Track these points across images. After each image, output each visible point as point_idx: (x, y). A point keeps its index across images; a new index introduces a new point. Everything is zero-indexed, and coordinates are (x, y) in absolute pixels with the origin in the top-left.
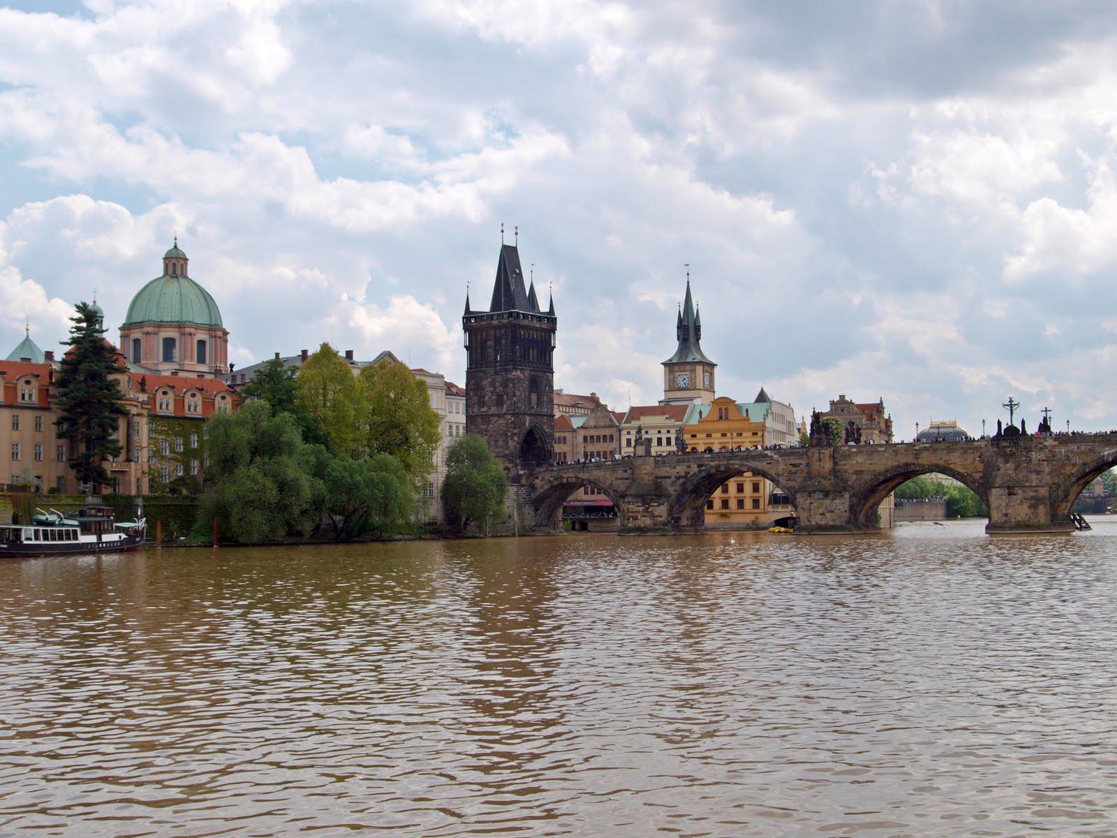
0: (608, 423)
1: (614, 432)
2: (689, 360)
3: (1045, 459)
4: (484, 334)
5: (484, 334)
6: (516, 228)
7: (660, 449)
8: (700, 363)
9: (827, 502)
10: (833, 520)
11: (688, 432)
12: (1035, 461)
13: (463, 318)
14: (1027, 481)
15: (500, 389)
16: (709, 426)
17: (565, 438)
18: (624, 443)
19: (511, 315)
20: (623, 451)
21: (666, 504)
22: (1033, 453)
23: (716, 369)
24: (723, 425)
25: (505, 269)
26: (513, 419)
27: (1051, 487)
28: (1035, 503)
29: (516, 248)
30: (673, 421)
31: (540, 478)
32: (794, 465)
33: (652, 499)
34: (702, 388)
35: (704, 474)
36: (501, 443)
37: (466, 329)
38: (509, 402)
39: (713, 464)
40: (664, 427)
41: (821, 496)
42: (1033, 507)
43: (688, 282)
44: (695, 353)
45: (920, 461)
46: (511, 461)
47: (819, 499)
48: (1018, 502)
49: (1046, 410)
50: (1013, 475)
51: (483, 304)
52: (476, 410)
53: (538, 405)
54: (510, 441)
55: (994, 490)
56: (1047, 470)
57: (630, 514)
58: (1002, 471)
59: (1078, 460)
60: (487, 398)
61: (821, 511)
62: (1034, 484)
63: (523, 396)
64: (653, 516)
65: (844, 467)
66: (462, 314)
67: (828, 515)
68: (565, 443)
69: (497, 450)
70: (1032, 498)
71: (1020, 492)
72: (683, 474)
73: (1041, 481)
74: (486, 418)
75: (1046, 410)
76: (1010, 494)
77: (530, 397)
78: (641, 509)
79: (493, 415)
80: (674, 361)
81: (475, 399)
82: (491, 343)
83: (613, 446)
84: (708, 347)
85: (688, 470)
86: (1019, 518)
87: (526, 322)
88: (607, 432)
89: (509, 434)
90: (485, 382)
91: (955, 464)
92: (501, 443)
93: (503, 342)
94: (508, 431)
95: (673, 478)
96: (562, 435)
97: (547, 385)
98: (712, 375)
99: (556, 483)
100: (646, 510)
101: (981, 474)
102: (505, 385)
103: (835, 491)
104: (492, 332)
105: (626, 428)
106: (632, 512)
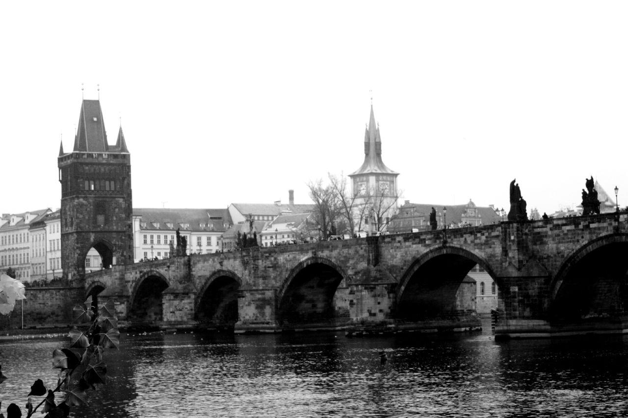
2: (366, 172)
3: (271, 266)
8: (372, 174)
9: (176, 302)
10: (182, 317)
12: (261, 268)
14: (254, 286)
21: (126, 303)
22: (260, 261)
23: (398, 177)
27: (276, 290)
33: (115, 299)
35: (143, 279)
36: (73, 255)
40: (285, 233)
41: (172, 297)
42: (260, 307)
43: (372, 106)
45: (224, 268)
47: (170, 300)
48: (247, 303)
50: (248, 280)
53: (105, 224)
54: (76, 253)
56: (273, 275)
59: (289, 266)
61: (171, 310)
62: (261, 288)
63: (87, 218)
67: (177, 313)
70: (259, 299)
71: (248, 294)
73: (267, 286)
79: (70, 233)
84: (390, 160)
86: (247, 317)
87: (89, 160)
89: (75, 248)
91: (237, 270)
97: (116, 208)
98: (392, 182)
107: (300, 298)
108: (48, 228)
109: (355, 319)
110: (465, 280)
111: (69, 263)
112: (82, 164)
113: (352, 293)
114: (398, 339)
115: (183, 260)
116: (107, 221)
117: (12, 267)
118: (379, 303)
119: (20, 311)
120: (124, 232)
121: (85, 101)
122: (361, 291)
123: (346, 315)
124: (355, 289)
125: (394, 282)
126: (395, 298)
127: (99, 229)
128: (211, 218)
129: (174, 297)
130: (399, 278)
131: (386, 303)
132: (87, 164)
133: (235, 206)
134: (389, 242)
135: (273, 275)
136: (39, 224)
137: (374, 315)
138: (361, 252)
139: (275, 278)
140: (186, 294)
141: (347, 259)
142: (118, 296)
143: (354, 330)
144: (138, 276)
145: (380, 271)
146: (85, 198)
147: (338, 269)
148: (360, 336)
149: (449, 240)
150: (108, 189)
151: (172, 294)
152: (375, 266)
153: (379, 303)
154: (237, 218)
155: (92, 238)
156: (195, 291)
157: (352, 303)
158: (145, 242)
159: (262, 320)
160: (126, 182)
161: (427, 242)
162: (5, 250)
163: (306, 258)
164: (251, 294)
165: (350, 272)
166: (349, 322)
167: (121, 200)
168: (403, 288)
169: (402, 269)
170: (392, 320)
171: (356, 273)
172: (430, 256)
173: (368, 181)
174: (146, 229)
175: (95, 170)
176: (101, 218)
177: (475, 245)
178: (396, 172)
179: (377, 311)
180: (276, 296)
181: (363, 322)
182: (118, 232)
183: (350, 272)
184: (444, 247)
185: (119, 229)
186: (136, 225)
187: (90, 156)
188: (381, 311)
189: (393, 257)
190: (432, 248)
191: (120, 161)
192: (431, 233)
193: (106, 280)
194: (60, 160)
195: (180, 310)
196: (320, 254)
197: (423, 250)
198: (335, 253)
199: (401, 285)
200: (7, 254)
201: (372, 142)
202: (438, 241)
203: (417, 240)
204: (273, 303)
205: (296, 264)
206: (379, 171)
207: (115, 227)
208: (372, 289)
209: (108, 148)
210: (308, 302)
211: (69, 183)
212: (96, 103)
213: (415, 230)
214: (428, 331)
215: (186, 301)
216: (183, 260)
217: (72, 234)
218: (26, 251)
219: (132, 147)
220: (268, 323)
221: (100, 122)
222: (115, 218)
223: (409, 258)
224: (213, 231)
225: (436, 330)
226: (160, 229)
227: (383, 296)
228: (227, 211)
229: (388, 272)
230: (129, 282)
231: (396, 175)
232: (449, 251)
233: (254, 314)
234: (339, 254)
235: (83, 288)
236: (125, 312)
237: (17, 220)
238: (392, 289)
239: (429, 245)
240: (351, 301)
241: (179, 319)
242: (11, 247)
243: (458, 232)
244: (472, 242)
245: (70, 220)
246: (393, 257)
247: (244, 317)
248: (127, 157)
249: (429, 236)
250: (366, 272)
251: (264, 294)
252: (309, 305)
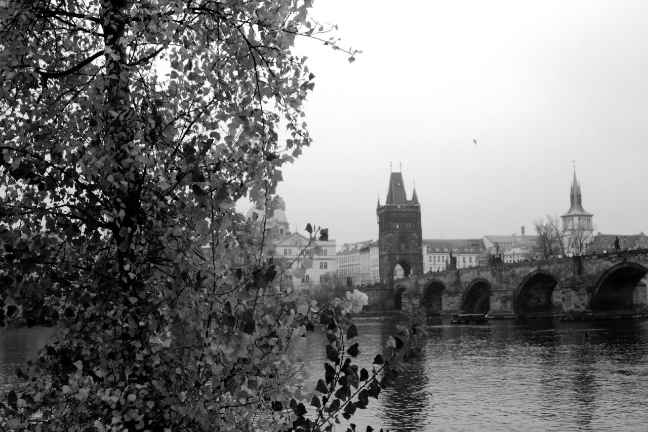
2: (572, 214)
8: (576, 215)
9: (450, 298)
14: (500, 288)
22: (504, 272)
23: (593, 217)
37: (378, 214)
45: (481, 277)
51: (383, 203)
53: (406, 250)
59: (522, 275)
62: (504, 289)
66: (376, 207)
67: (451, 305)
70: (503, 297)
71: (496, 294)
77: (400, 246)
84: (587, 205)
86: (496, 308)
97: (412, 239)
98: (589, 220)
100: (410, 302)
105: (507, 255)
107: (531, 296)
108: (371, 252)
109: (566, 309)
110: (639, 284)
112: (391, 212)
113: (564, 292)
114: (596, 322)
116: (407, 247)
117: (350, 276)
118: (582, 299)
120: (417, 254)
122: (570, 292)
123: (560, 307)
124: (566, 290)
125: (591, 285)
126: (592, 296)
128: (472, 245)
130: (595, 283)
131: (586, 299)
132: (394, 212)
133: (487, 237)
134: (588, 260)
135: (512, 281)
136: (366, 249)
137: (579, 307)
138: (570, 266)
139: (513, 283)
140: (456, 293)
141: (560, 270)
143: (565, 317)
144: (426, 281)
145: (582, 278)
146: (393, 233)
147: (554, 277)
148: (569, 320)
149: (628, 258)
150: (407, 227)
152: (579, 275)
153: (582, 299)
154: (488, 245)
155: (398, 258)
156: (462, 291)
157: (563, 299)
158: (430, 260)
159: (505, 310)
160: (418, 223)
161: (613, 259)
162: (346, 266)
163: (533, 270)
165: (562, 279)
166: (562, 311)
167: (415, 235)
168: (597, 289)
170: (590, 311)
171: (566, 280)
172: (616, 268)
173: (573, 220)
174: (431, 252)
176: (403, 246)
177: (646, 261)
178: (591, 214)
179: (580, 305)
180: (514, 294)
181: (571, 312)
182: (413, 254)
183: (562, 279)
184: (625, 262)
185: (415, 253)
186: (425, 250)
188: (583, 304)
189: (591, 269)
190: (616, 263)
191: (414, 210)
192: (616, 253)
193: (407, 284)
194: (378, 210)
195: (453, 303)
196: (542, 268)
197: (611, 265)
198: (552, 267)
199: (596, 287)
200: (347, 268)
201: (575, 194)
202: (620, 259)
203: (606, 258)
204: (512, 299)
205: (527, 274)
206: (580, 214)
208: (576, 290)
209: (407, 202)
210: (535, 298)
213: (605, 252)
214: (615, 317)
215: (456, 298)
217: (385, 255)
218: (358, 266)
219: (421, 201)
220: (509, 312)
221: (402, 186)
223: (601, 270)
224: (473, 253)
225: (620, 317)
226: (439, 252)
227: (584, 295)
228: (482, 241)
229: (587, 279)
230: (420, 285)
231: (591, 216)
232: (628, 265)
234: (555, 267)
235: (393, 289)
236: (418, 303)
237: (353, 247)
238: (590, 290)
239: (614, 262)
240: (563, 298)
241: (452, 309)
242: (349, 263)
243: (634, 253)
244: (644, 259)
246: (591, 269)
248: (418, 208)
249: (614, 256)
250: (573, 279)
251: (506, 293)
252: (536, 301)
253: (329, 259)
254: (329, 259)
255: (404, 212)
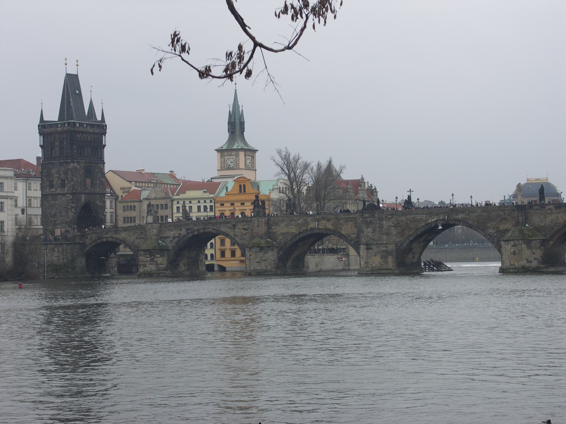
0: (164, 195)
1: (168, 202)
2: (235, 147)
4: (53, 137)
5: (53, 137)
6: (77, 61)
7: (199, 214)
8: (242, 149)
9: (260, 254)
10: (266, 266)
11: (218, 202)
13: (39, 126)
14: (380, 240)
15: (63, 176)
16: (232, 198)
17: (135, 207)
18: (175, 210)
19: (69, 123)
20: (174, 215)
22: (385, 221)
24: (242, 197)
25: (68, 91)
26: (71, 197)
28: (385, 255)
29: (77, 76)
30: (208, 194)
31: (89, 238)
32: (245, 229)
34: (244, 168)
35: (190, 235)
36: (64, 214)
37: (40, 134)
38: (69, 185)
39: (195, 228)
41: (258, 250)
43: (236, 90)
44: (239, 142)
46: (70, 227)
47: (256, 252)
48: (374, 254)
49: (410, 191)
51: (52, 115)
52: (47, 190)
53: (91, 188)
54: (70, 213)
55: (362, 246)
57: (141, 263)
58: (365, 233)
60: (54, 182)
61: (257, 260)
62: (385, 242)
64: (157, 264)
65: (274, 230)
66: (38, 122)
68: (134, 210)
69: (61, 219)
70: (383, 251)
72: (177, 235)
74: (54, 196)
75: (410, 191)
76: (367, 249)
77: (85, 181)
78: (149, 259)
79: (58, 194)
80: (224, 148)
81: (47, 183)
82: (57, 144)
83: (168, 212)
85: (181, 232)
86: (374, 265)
87: (81, 129)
88: (163, 202)
89: (69, 207)
90: (54, 171)
92: (64, 214)
93: (65, 143)
94: (68, 205)
95: (171, 238)
96: (132, 204)
97: (99, 172)
98: (253, 157)
99: (99, 241)
100: (152, 260)
101: (356, 235)
102: (66, 173)
103: (268, 247)
104: (58, 136)
105: (176, 199)
106: (143, 261)
111: (55, 221)
113: (514, 246)
115: (264, 220)
116: (93, 184)
118: (534, 253)
119: (43, 263)
121: (68, 75)
122: (521, 244)
127: (87, 191)
129: (260, 250)
131: (539, 253)
137: (531, 262)
140: (270, 247)
142: (159, 250)
151: (258, 247)
153: (534, 253)
164: (377, 247)
168: (552, 242)
169: (553, 229)
173: (237, 156)
175: (84, 138)
178: (256, 148)
187: (81, 125)
188: (535, 259)
201: (237, 121)
206: (246, 148)
207: (98, 190)
211: (57, 149)
212: (76, 76)
216: (264, 220)
220: (391, 269)
221: (80, 94)
222: (98, 182)
231: (255, 151)
233: (379, 263)
245: (59, 182)
247: (371, 265)
251: (387, 247)
253: (6, 197)
254: (6, 197)
255: (90, 133)
